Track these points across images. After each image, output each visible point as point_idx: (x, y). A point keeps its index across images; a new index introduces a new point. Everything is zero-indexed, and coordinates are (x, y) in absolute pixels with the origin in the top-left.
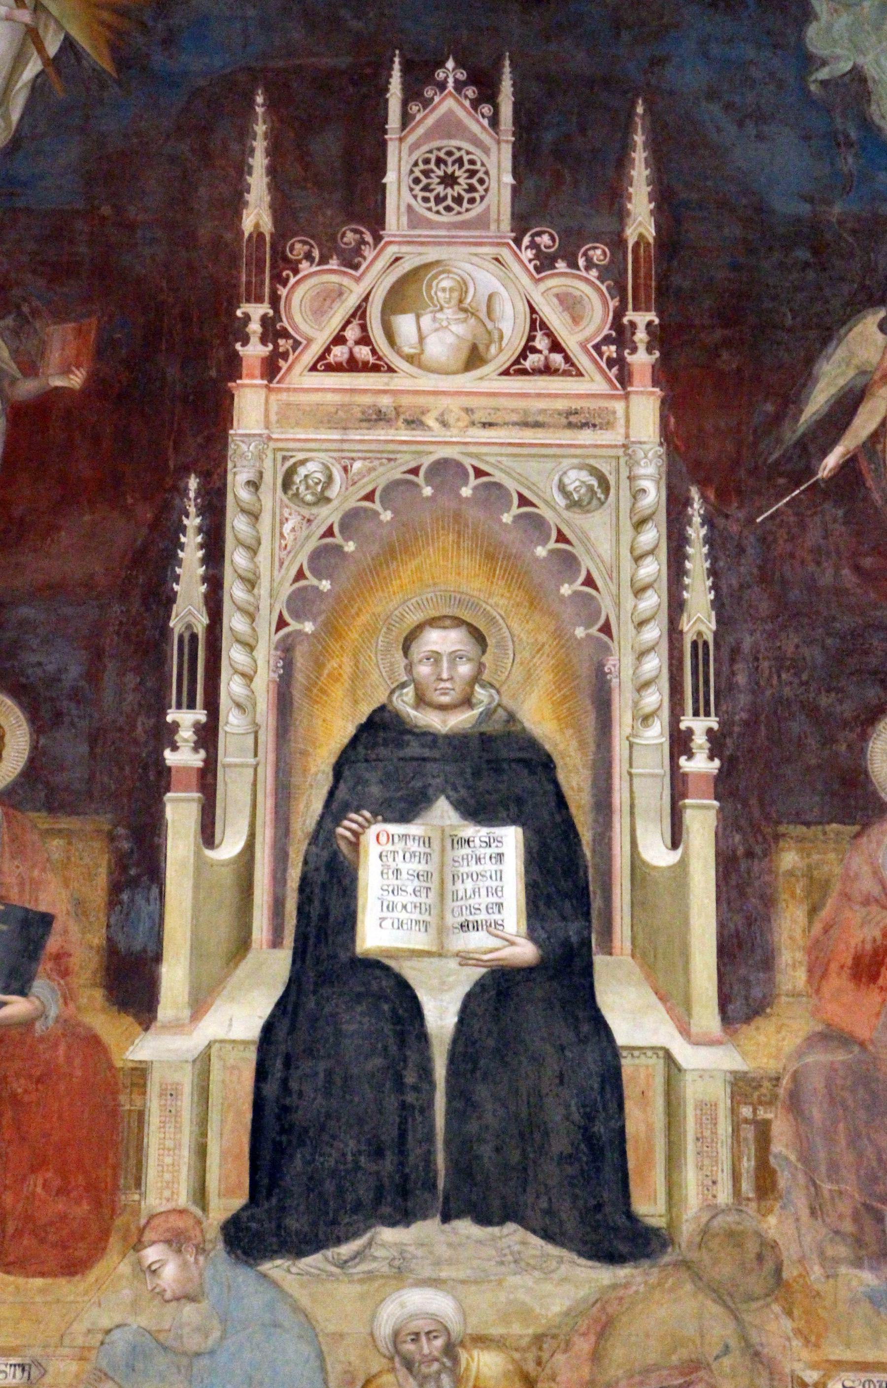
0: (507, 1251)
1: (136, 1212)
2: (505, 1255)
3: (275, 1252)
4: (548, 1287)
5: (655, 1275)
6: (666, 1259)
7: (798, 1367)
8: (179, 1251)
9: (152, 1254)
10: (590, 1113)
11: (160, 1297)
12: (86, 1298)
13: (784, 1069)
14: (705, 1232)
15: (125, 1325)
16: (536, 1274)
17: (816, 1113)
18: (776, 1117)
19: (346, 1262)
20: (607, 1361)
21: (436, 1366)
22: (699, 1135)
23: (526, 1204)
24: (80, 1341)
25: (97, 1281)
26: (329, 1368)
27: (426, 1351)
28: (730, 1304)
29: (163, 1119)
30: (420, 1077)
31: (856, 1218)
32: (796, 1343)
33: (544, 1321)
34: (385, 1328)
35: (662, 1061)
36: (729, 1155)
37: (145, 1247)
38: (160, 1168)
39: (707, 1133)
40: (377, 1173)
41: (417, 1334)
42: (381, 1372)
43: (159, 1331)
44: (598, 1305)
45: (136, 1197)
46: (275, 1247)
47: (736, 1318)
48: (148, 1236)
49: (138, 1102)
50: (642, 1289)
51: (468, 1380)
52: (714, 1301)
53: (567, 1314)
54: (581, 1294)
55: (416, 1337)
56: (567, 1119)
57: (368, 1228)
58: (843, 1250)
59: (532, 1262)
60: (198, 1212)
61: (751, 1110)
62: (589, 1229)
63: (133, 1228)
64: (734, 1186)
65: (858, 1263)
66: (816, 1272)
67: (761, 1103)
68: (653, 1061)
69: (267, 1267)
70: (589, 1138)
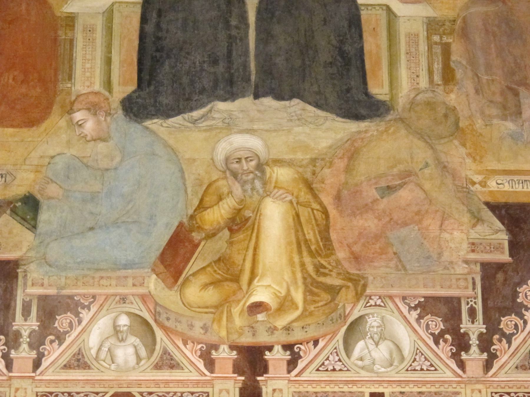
0: (293, 114)
1: (69, 93)
2: (292, 116)
3: (153, 115)
4: (319, 133)
5: (382, 126)
6: (389, 117)
7: (469, 173)
8: (95, 114)
9: (78, 116)
10: (342, 40)
11: (84, 139)
12: (39, 139)
13: (458, 15)
14: (413, 104)
15: (64, 154)
16: (311, 126)
17: (478, 39)
18: (454, 41)
19: (196, 120)
20: (355, 172)
21: (251, 176)
22: (408, 51)
23: (305, 90)
24: (36, 163)
25: (45, 130)
26: (186, 176)
27: (245, 168)
28: (429, 141)
29: (85, 44)
30: (240, 22)
31: (502, 93)
32: (469, 161)
33: (317, 151)
34: (220, 156)
35: (385, 12)
36: (426, 61)
37: (75, 112)
38: (83, 70)
39: (413, 50)
40: (215, 73)
41: (240, 159)
42: (218, 179)
43: (84, 157)
44: (349, 142)
45: (69, 85)
46: (153, 113)
47: (432, 148)
48: (76, 106)
49: (70, 34)
50: (375, 133)
51: (270, 183)
52: (419, 139)
53: (330, 147)
54: (339, 136)
55: (239, 161)
56: (329, 43)
57: (210, 102)
58: (494, 111)
59: (309, 120)
60: (107, 94)
61: (439, 37)
62: (342, 102)
63: (67, 101)
64: (429, 78)
65: (504, 118)
66: (479, 123)
67: (444, 34)
68: (380, 11)
69: (148, 123)
70: (342, 53)
